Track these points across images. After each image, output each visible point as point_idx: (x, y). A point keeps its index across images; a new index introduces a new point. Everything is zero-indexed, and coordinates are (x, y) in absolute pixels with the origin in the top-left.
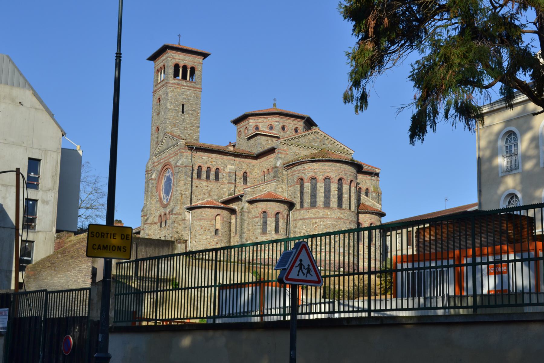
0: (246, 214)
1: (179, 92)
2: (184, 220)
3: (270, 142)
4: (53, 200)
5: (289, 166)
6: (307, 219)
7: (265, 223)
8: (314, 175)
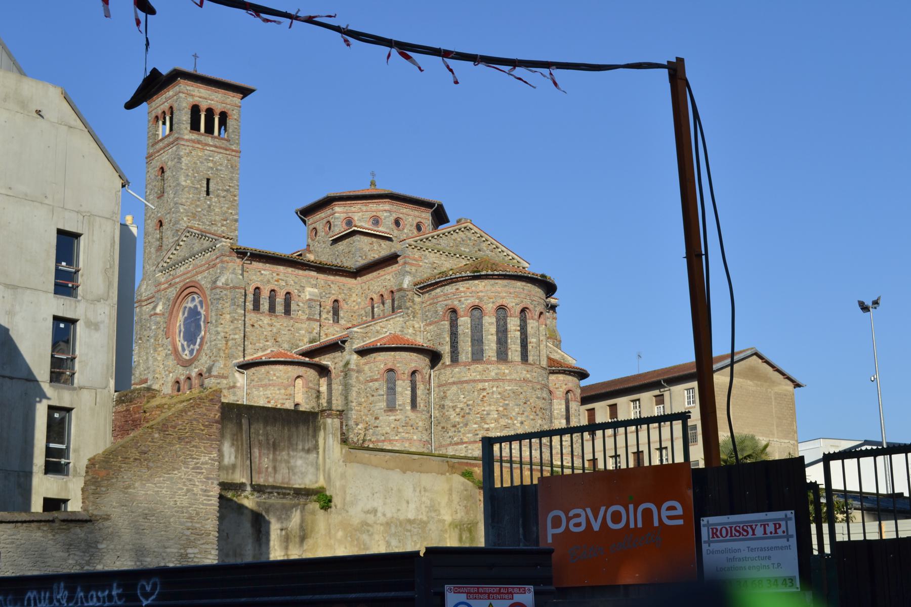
0: (354, 375)
1: (200, 157)
2: (234, 387)
3: (376, 247)
4: (107, 321)
5: (425, 287)
6: (466, 382)
7: (392, 390)
8: (477, 302)
